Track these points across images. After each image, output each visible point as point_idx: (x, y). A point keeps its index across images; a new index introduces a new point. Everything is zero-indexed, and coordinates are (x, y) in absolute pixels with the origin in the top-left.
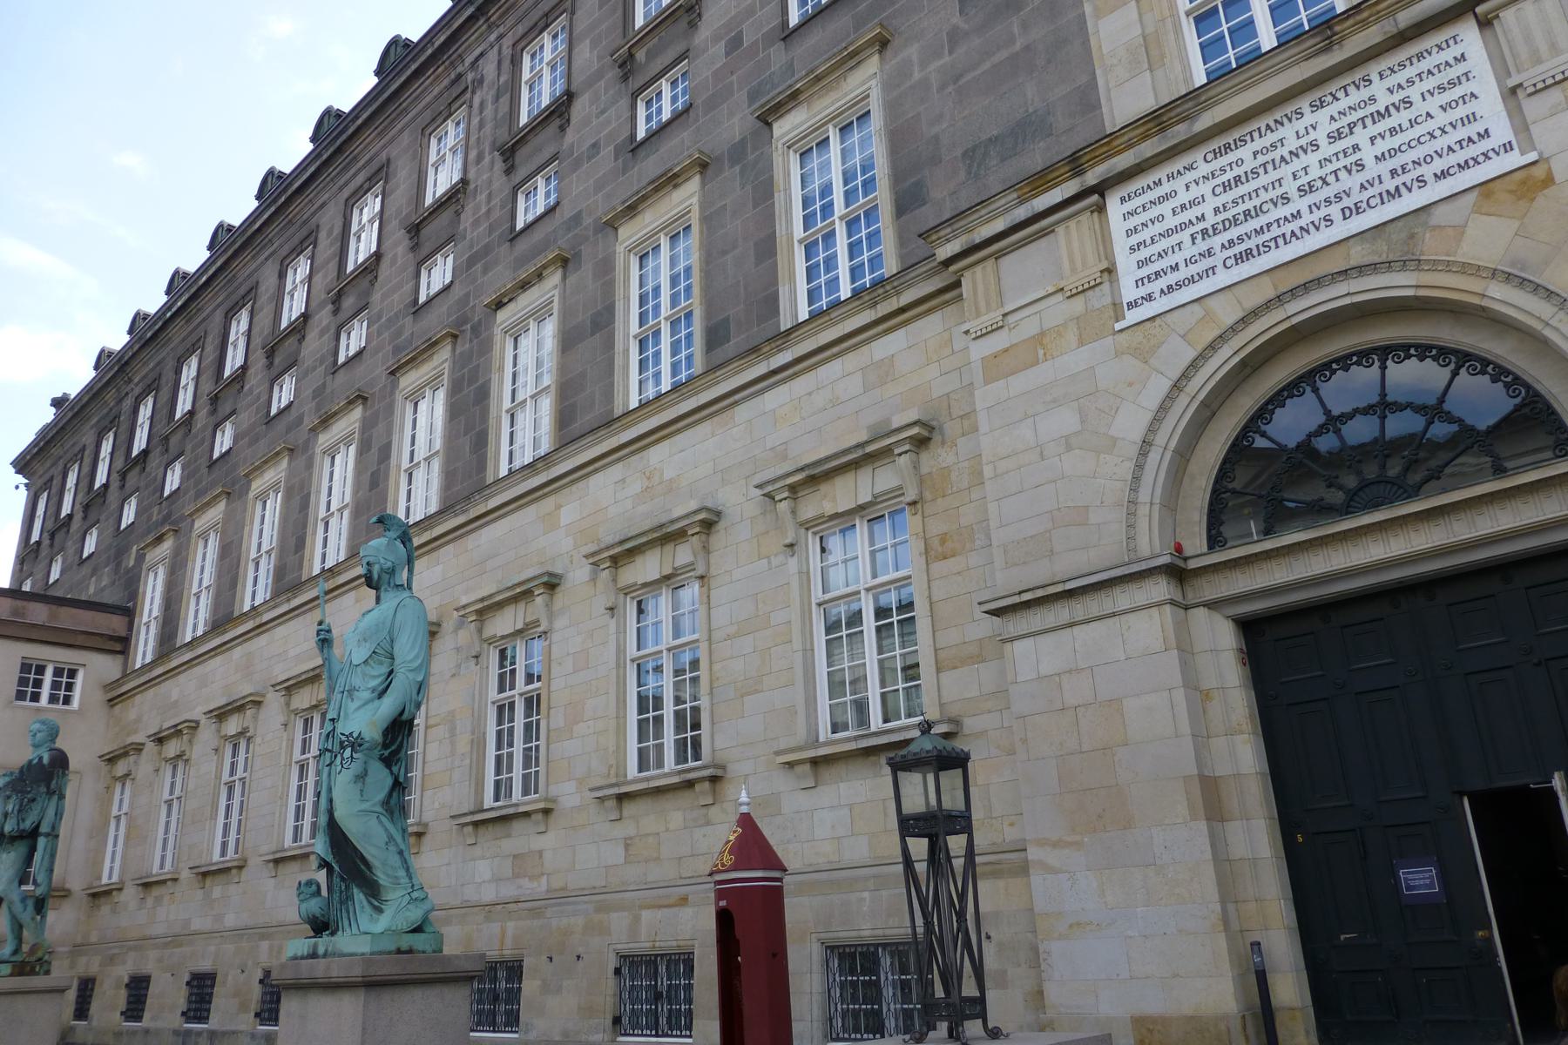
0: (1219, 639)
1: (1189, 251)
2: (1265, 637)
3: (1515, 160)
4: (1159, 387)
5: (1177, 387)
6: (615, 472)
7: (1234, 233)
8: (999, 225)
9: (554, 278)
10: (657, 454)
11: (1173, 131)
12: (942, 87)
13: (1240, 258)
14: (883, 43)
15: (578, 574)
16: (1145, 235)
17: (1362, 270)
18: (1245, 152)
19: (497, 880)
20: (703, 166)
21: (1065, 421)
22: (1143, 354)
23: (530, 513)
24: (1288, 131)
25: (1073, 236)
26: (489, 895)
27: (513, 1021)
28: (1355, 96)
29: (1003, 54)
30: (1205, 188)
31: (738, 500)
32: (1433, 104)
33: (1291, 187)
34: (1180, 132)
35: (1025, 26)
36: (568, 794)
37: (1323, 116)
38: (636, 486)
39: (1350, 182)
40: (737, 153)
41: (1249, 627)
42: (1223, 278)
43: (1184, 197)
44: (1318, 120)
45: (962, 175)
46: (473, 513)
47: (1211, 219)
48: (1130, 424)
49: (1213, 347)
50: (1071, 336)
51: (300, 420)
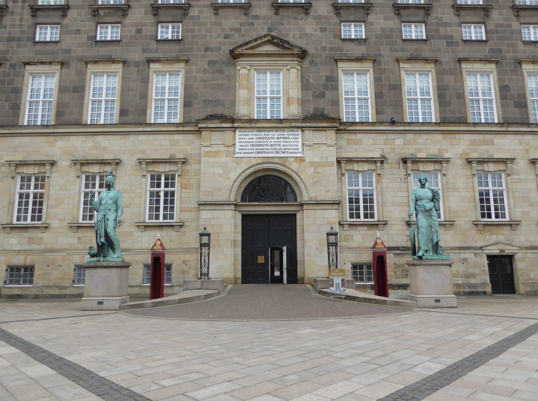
0: (239, 217)
1: (249, 147)
2: (246, 218)
3: (300, 155)
4: (239, 171)
5: (243, 172)
6: (83, 138)
7: (258, 147)
8: (214, 126)
9: (59, 67)
10: (99, 138)
12: (200, 81)
13: (259, 153)
14: (187, 61)
15: (64, 163)
16: (242, 140)
17: (277, 163)
18: (263, 133)
19: (20, 244)
20: (124, 62)
21: (220, 171)
22: (238, 163)
23: (43, 139)
24: (270, 133)
25: (228, 134)
26: (17, 248)
27: (31, 282)
28: (282, 133)
29: (216, 82)
30: (255, 137)
31: (129, 161)
32: (293, 140)
33: (269, 144)
34: (253, 125)
35: (222, 79)
36: (54, 223)
37: (276, 133)
39: (278, 147)
40: (137, 64)
41: (244, 216)
42: (254, 155)
43: (250, 137)
44: (276, 134)
45: (202, 105)
46: (13, 131)
47: (254, 143)
48: (233, 175)
49: (251, 167)
50: (224, 154)
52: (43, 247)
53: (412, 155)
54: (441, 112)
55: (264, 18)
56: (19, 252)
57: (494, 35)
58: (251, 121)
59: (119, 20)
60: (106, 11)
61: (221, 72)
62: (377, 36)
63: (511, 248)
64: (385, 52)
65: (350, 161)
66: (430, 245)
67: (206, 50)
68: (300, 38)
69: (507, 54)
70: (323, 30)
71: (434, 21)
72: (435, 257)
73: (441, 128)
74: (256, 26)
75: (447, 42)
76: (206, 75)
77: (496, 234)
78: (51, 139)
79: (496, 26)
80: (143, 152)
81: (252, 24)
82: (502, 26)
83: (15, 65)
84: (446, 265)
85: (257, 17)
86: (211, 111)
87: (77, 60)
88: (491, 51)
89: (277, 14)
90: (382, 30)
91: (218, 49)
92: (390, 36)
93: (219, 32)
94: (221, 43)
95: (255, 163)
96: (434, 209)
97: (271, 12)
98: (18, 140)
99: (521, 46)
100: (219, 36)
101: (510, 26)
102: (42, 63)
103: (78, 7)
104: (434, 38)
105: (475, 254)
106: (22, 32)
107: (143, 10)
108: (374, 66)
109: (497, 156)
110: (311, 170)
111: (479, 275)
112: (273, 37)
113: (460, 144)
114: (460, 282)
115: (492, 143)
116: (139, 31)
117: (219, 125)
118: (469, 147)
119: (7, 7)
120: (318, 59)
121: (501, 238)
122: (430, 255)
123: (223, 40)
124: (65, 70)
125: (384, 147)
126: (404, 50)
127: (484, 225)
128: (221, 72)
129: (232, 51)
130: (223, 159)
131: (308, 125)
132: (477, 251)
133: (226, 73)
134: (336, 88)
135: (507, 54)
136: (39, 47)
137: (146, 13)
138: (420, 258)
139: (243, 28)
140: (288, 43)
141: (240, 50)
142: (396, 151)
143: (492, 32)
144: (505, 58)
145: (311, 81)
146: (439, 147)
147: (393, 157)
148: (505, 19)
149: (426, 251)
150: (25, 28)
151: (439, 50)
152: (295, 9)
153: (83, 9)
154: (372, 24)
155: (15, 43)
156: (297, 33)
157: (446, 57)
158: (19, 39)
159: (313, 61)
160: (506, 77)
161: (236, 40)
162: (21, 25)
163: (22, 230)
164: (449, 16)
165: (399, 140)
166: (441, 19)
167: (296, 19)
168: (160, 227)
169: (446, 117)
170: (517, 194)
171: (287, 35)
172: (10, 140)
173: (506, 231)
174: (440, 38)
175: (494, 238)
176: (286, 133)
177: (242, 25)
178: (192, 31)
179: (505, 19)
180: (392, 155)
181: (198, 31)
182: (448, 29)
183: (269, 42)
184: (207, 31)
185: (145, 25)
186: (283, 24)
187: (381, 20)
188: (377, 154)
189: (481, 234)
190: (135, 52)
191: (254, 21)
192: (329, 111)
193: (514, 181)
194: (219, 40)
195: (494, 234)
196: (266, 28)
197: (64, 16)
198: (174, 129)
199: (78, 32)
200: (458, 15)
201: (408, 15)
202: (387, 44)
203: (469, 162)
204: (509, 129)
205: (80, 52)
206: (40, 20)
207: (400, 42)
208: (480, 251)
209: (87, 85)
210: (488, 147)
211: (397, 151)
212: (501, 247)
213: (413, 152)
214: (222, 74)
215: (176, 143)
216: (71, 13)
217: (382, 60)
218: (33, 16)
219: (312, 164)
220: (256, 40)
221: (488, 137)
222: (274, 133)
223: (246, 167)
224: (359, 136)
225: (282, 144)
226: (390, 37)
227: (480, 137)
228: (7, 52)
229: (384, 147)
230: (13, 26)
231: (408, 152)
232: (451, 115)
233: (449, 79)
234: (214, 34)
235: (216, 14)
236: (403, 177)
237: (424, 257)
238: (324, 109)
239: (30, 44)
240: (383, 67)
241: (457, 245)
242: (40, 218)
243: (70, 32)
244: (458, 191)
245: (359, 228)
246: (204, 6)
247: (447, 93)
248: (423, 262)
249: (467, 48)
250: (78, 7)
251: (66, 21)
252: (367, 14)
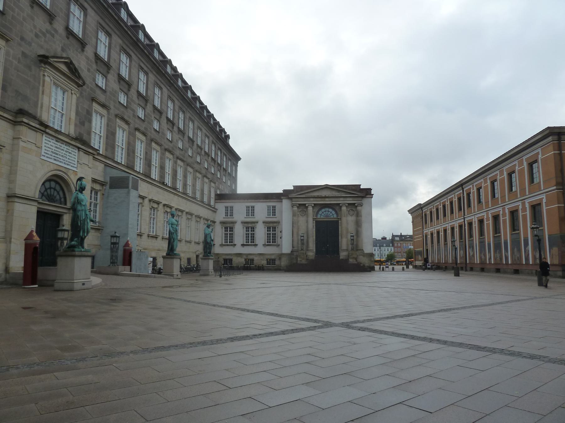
13: (55, 160)
18: (59, 144)
25: (39, 135)
30: (54, 145)
34: (57, 135)
37: (66, 147)
134: (90, 121)
183: (65, 63)
192: (85, 137)
242: (275, 242)
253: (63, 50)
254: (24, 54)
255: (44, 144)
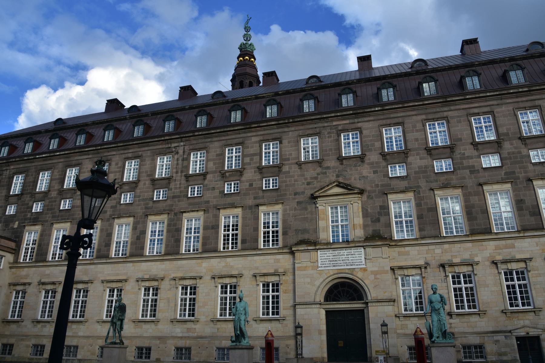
0: (323, 312)
2: (329, 313)
3: (364, 266)
4: (321, 280)
5: (324, 280)
6: (218, 260)
8: (303, 249)
9: (202, 213)
10: (229, 260)
11: (328, 245)
15: (207, 278)
17: (347, 273)
18: (336, 252)
19: (182, 332)
21: (308, 280)
22: (320, 274)
23: (194, 261)
24: (342, 252)
25: (313, 254)
26: (180, 335)
30: (331, 255)
31: (248, 274)
32: (358, 256)
34: (329, 247)
35: (307, 214)
36: (203, 319)
37: (346, 251)
38: (223, 264)
40: (250, 207)
41: (326, 311)
42: (331, 268)
43: (328, 255)
44: (345, 252)
46: (177, 257)
48: (317, 283)
49: (329, 277)
50: (311, 268)
51: (106, 212)
52: (195, 335)
53: (449, 260)
54: (470, 225)
55: (334, 168)
56: (181, 338)
57: (508, 161)
58: (328, 243)
59: (238, 178)
60: (230, 173)
61: (306, 209)
62: (416, 173)
63: (536, 330)
64: (423, 183)
65: (401, 268)
66: (440, 333)
67: (296, 194)
68: (360, 180)
69: (520, 175)
70: (375, 172)
71: (459, 156)
72: (444, 341)
73: (470, 239)
74: (328, 174)
75: (470, 171)
76: (296, 212)
77: (523, 320)
78: (199, 261)
79: (509, 153)
80: (257, 268)
81: (325, 173)
82: (513, 153)
83: (177, 213)
84: (451, 346)
85: (328, 168)
86: (300, 237)
87: (213, 207)
88: (506, 173)
89: (342, 164)
90: (419, 167)
91: (303, 193)
92: (427, 172)
93: (304, 181)
94: (304, 189)
95: (332, 274)
96: (442, 308)
97: (337, 164)
98: (180, 262)
99: (531, 167)
100: (304, 183)
101: (520, 153)
102: (193, 211)
103: (213, 172)
104: (459, 169)
105: (506, 337)
106: (181, 192)
107: (253, 170)
108: (415, 195)
109: (518, 256)
110: (372, 277)
111: (509, 353)
112: (340, 183)
113: (486, 249)
114: (494, 359)
115: (513, 247)
116: (251, 185)
117: (306, 248)
118: (495, 251)
119: (173, 177)
120: (373, 194)
121: (527, 323)
122: (441, 340)
123: (306, 186)
124: (206, 215)
125: (426, 256)
126: (437, 181)
127: (511, 312)
128: (306, 209)
129: (312, 195)
130: (310, 272)
131: (367, 244)
132: (507, 334)
133: (309, 210)
135: (520, 175)
136: (191, 201)
137: (255, 172)
138: (433, 342)
139: (319, 176)
140: (350, 186)
141: (317, 194)
142: (436, 258)
143: (506, 159)
144: (518, 178)
145: (369, 210)
146: (470, 253)
147: (434, 263)
148: (515, 148)
149: (438, 337)
150: (182, 189)
151: (464, 178)
152: (354, 159)
153: (216, 173)
154: (411, 164)
155: (177, 199)
156: (357, 176)
157: (470, 182)
158: (179, 197)
159: (370, 196)
160: (521, 193)
161: (315, 185)
162: (180, 187)
163: (183, 323)
164: (470, 151)
165: (438, 250)
166: (464, 154)
167: (355, 166)
168: (270, 320)
169: (474, 229)
170: (538, 286)
171: (350, 179)
172: (175, 262)
173: (531, 316)
174: (464, 168)
175: (521, 323)
176: (352, 251)
177: (318, 174)
178: (286, 182)
179: (515, 148)
180: (433, 261)
181: (289, 181)
182: (470, 160)
183: (337, 186)
184: (295, 181)
185: (255, 180)
186: (346, 171)
187: (417, 161)
188: (421, 262)
189: (510, 320)
190: (249, 199)
191: (327, 171)
192: (383, 232)
193: (534, 275)
194: (304, 186)
195: (521, 320)
196: (335, 175)
197: (205, 179)
198: (276, 251)
199: (214, 189)
200: (477, 149)
201: (438, 154)
202: (424, 178)
203: (495, 263)
204: (526, 235)
205: (214, 202)
206: (191, 183)
207: (433, 175)
208: (510, 334)
209: (220, 224)
210: (511, 250)
211: (436, 258)
212: (528, 329)
213: (450, 258)
214: (306, 210)
215: (278, 261)
216: (209, 177)
217: (421, 190)
218: (187, 181)
219: (372, 272)
220: (328, 186)
221: (509, 242)
222: (344, 251)
223: (326, 277)
224: (407, 249)
225: (350, 259)
226: (426, 172)
227: (503, 242)
228: (172, 205)
229: (426, 256)
230: (176, 188)
231: (445, 259)
232: (478, 227)
233: (474, 200)
234: (300, 183)
235: (301, 168)
236: (443, 278)
237: (436, 342)
238: (380, 230)
239: (185, 199)
240: (422, 195)
241: (491, 329)
243: (208, 189)
244: (488, 287)
245: (412, 319)
246: (292, 164)
247: (473, 210)
248: (435, 345)
249: (486, 174)
250: (213, 172)
251: (206, 182)
252: (407, 157)
253: (338, 176)
254: (299, 203)
255: (319, 258)
